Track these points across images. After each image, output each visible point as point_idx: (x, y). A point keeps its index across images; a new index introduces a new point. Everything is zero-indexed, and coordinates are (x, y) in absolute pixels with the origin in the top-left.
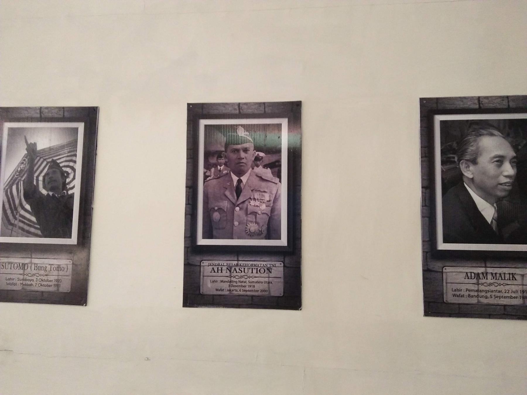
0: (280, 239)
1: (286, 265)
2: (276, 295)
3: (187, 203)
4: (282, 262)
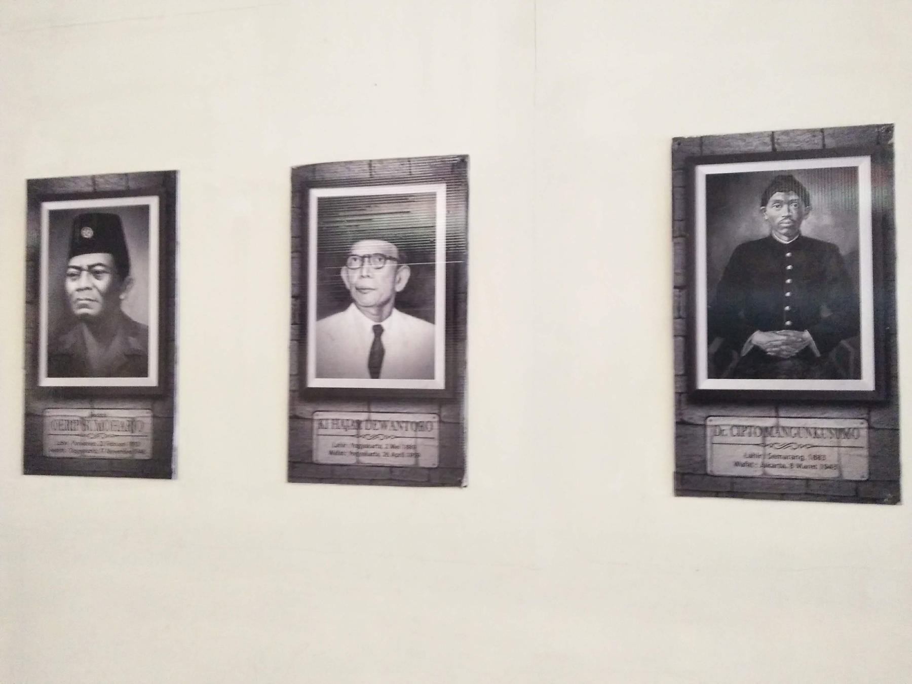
2: (854, 479)
3: (676, 315)
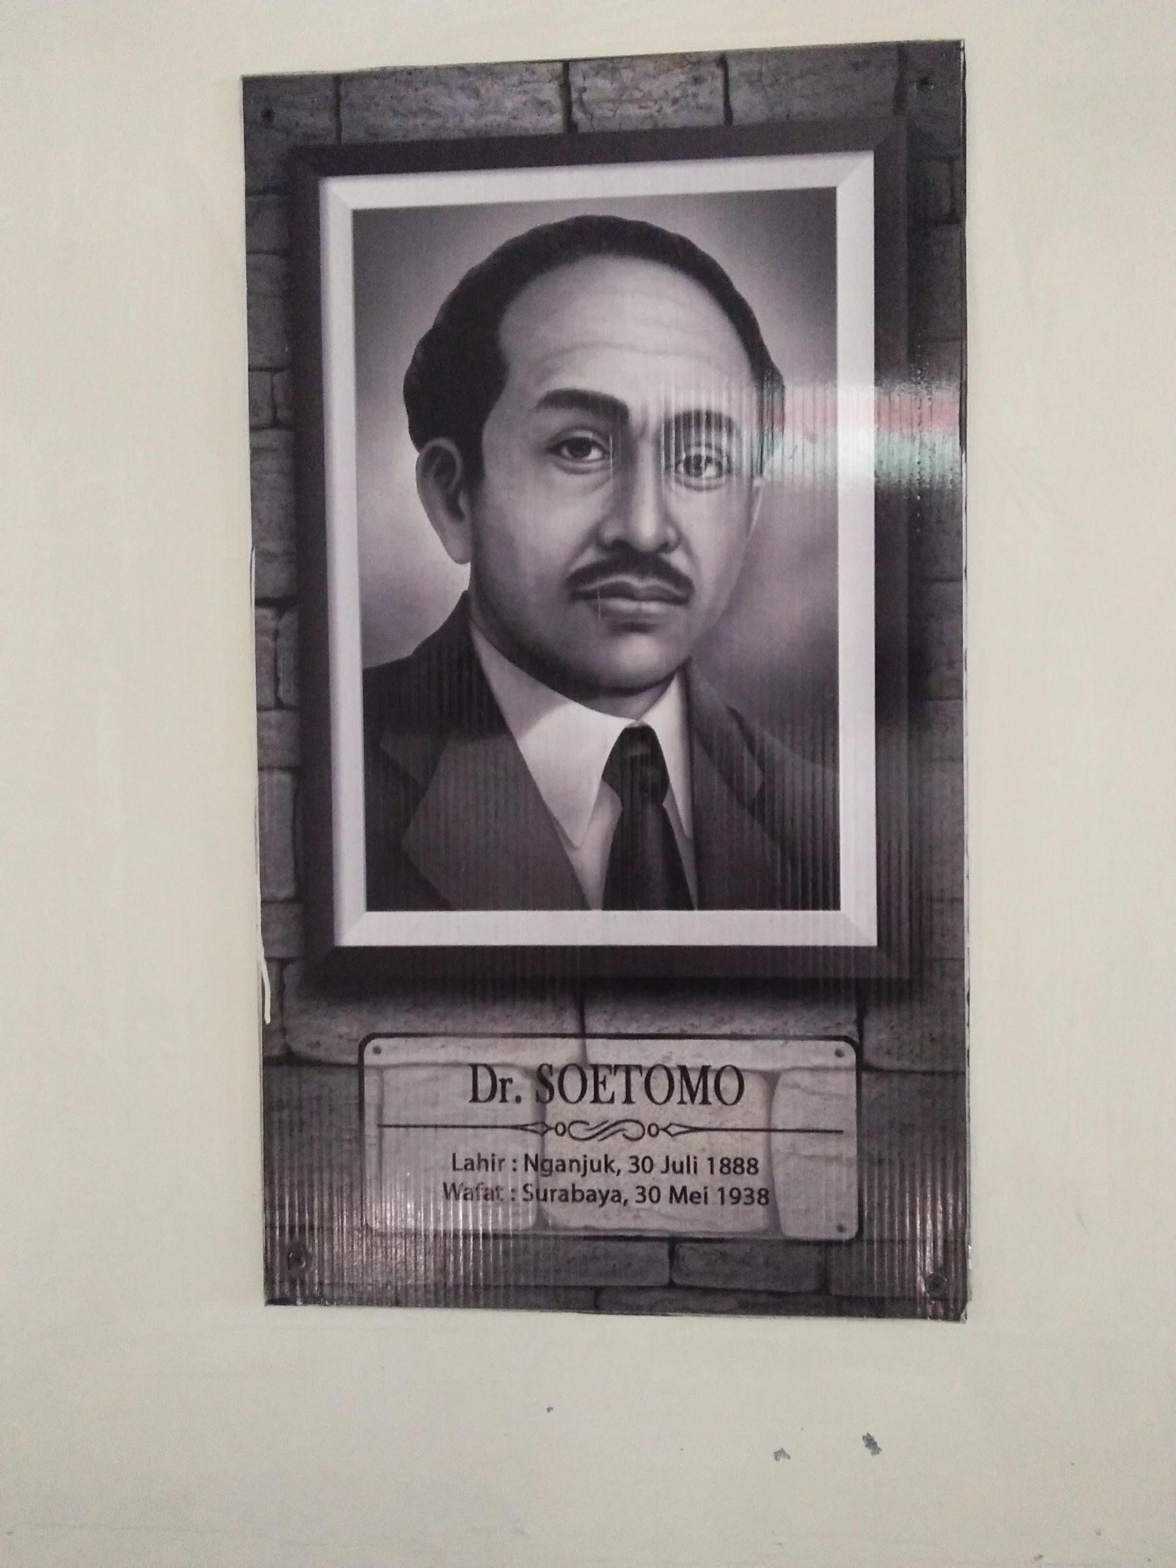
0: (837, 907)
1: (871, 1057)
2: (812, 1235)
3: (270, 700)
4: (847, 1039)
